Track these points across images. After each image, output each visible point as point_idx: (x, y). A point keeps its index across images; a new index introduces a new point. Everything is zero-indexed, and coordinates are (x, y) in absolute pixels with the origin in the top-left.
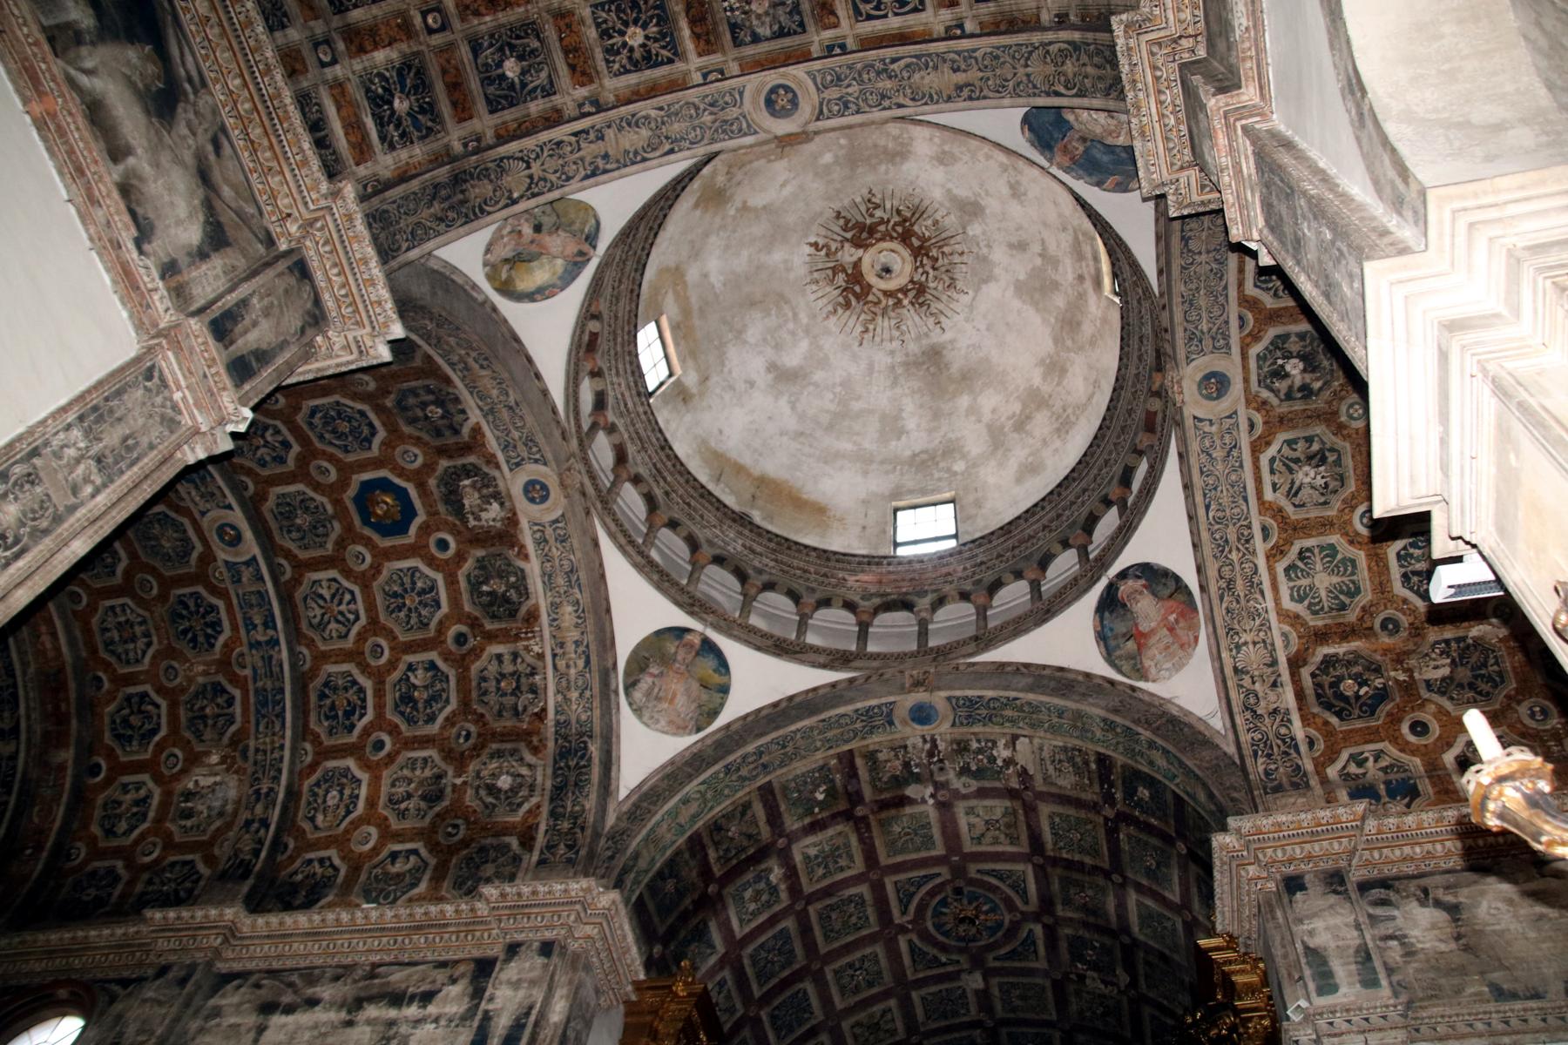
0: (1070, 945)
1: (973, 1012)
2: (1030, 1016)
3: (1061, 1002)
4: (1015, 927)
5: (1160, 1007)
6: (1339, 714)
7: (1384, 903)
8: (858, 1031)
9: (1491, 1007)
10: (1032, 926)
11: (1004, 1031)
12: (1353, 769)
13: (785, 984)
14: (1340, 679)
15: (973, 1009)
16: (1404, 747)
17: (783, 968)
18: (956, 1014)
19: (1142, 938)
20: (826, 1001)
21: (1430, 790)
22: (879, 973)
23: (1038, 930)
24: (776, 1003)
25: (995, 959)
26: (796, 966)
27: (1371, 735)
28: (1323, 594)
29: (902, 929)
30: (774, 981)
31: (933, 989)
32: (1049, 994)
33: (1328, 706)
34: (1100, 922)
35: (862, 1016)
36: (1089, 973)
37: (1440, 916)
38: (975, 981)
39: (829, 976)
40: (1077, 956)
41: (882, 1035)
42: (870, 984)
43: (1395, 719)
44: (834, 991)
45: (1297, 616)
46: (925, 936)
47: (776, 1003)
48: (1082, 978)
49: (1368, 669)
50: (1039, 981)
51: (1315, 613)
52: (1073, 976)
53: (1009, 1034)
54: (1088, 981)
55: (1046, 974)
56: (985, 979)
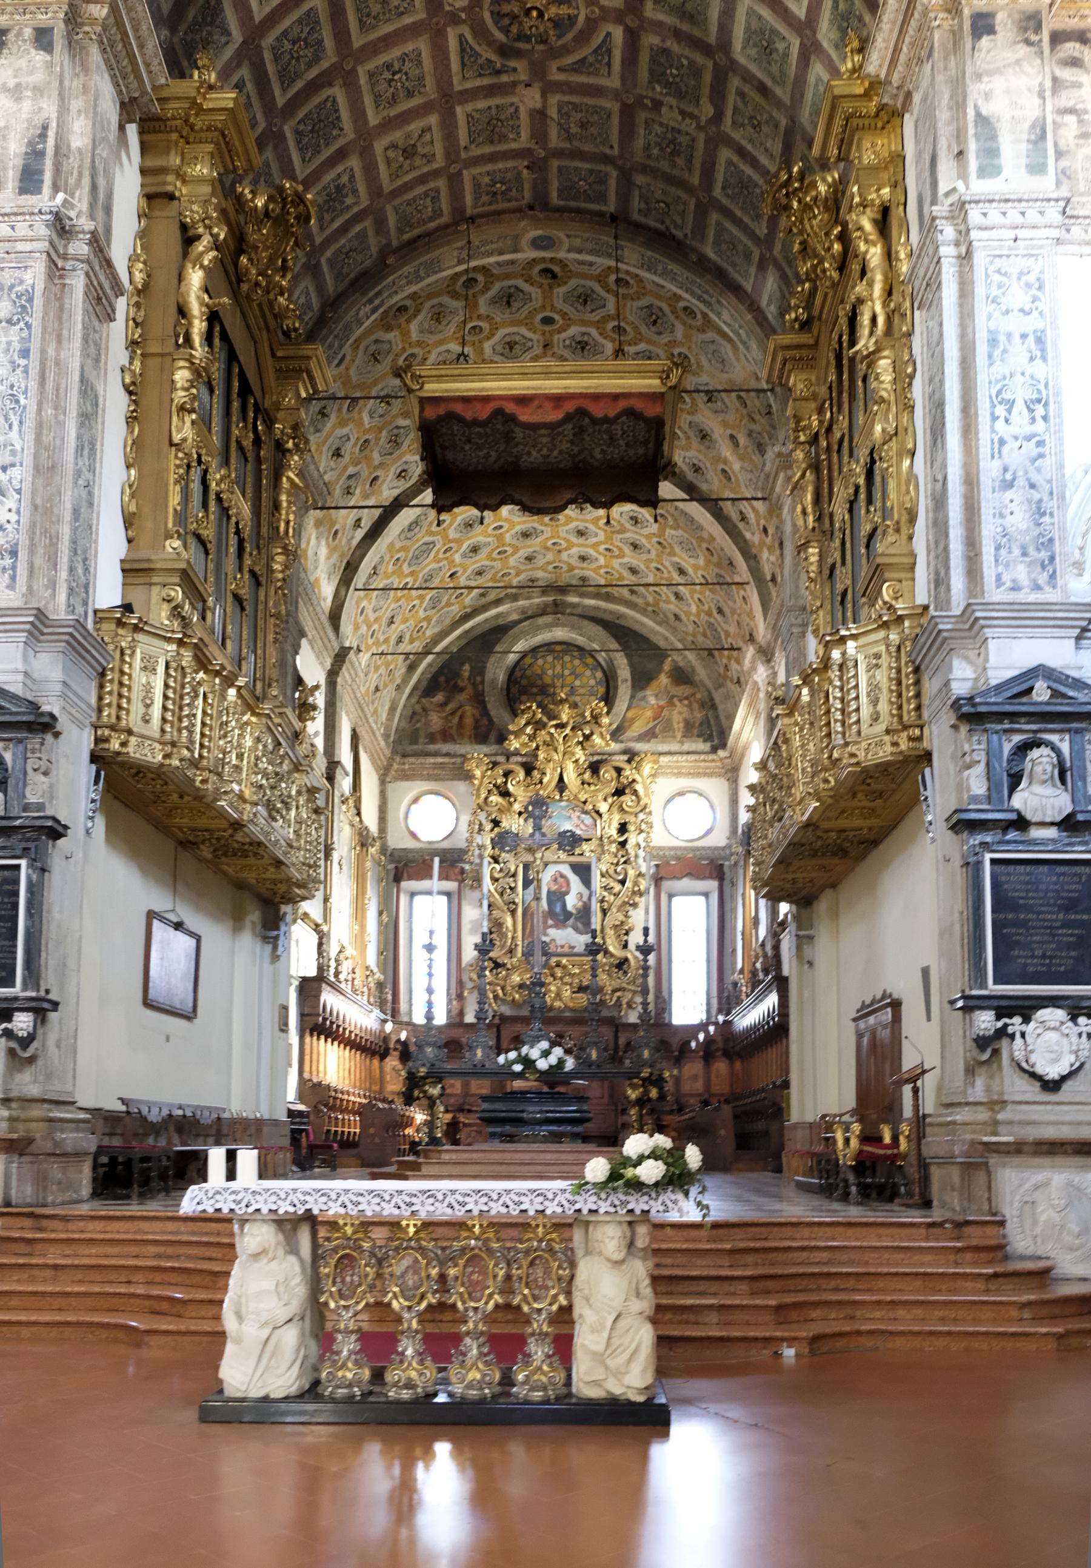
0: (653, 59)
1: (524, 139)
2: (588, 147)
3: (628, 132)
4: (592, 25)
5: (741, 152)
8: (391, 154)
10: (611, 28)
11: (555, 163)
13: (314, 87)
15: (525, 134)
17: (309, 65)
18: (503, 138)
19: (742, 60)
20: (358, 113)
22: (421, 79)
23: (618, 34)
24: (301, 114)
25: (559, 69)
26: (325, 64)
29: (454, 19)
30: (300, 84)
31: (481, 104)
32: (615, 120)
34: (697, 32)
35: (397, 136)
36: (667, 100)
38: (530, 98)
39: (363, 80)
40: (656, 76)
41: (418, 161)
42: (410, 94)
44: (368, 100)
46: (479, 30)
47: (301, 114)
48: (657, 105)
50: (607, 103)
52: (648, 102)
53: (560, 169)
54: (664, 110)
55: (616, 95)
56: (544, 95)
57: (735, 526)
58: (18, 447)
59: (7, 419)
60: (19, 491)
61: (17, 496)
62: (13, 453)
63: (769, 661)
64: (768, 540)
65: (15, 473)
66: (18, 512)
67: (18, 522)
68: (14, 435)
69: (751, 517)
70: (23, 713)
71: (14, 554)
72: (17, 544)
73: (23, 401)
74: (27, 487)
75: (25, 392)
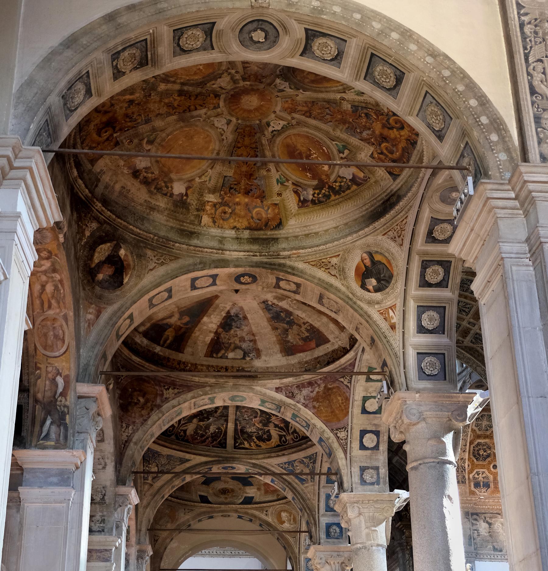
6: (477, 459)
7: (476, 520)
9: (492, 552)
12: (476, 476)
14: (480, 449)
16: (490, 472)
21: (493, 487)
27: (483, 467)
28: (483, 426)
33: (475, 456)
37: (487, 525)
43: (490, 463)
45: (475, 430)
49: (487, 448)
51: (480, 430)
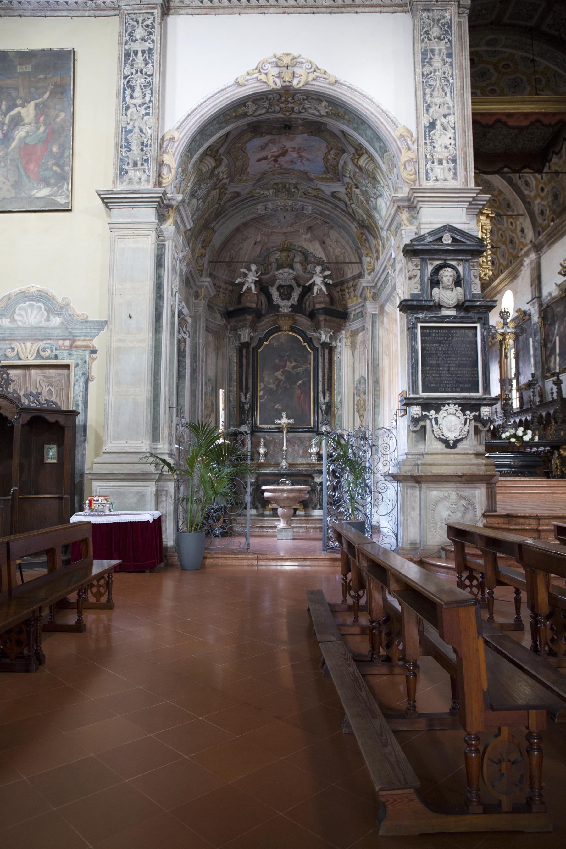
57: (519, 188)
58: (451, 105)
59: (443, 90)
60: (454, 128)
61: (453, 131)
62: (449, 108)
63: (537, 251)
64: (543, 195)
65: (451, 118)
66: (455, 139)
67: (455, 145)
68: (448, 98)
69: (533, 183)
70: (474, 245)
71: (454, 161)
72: (455, 156)
73: (451, 81)
74: (458, 126)
75: (452, 76)
